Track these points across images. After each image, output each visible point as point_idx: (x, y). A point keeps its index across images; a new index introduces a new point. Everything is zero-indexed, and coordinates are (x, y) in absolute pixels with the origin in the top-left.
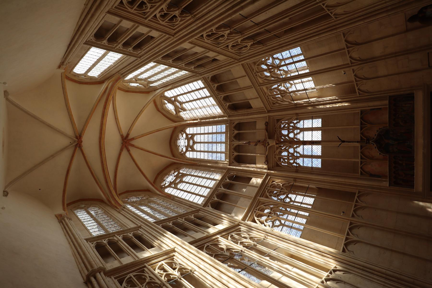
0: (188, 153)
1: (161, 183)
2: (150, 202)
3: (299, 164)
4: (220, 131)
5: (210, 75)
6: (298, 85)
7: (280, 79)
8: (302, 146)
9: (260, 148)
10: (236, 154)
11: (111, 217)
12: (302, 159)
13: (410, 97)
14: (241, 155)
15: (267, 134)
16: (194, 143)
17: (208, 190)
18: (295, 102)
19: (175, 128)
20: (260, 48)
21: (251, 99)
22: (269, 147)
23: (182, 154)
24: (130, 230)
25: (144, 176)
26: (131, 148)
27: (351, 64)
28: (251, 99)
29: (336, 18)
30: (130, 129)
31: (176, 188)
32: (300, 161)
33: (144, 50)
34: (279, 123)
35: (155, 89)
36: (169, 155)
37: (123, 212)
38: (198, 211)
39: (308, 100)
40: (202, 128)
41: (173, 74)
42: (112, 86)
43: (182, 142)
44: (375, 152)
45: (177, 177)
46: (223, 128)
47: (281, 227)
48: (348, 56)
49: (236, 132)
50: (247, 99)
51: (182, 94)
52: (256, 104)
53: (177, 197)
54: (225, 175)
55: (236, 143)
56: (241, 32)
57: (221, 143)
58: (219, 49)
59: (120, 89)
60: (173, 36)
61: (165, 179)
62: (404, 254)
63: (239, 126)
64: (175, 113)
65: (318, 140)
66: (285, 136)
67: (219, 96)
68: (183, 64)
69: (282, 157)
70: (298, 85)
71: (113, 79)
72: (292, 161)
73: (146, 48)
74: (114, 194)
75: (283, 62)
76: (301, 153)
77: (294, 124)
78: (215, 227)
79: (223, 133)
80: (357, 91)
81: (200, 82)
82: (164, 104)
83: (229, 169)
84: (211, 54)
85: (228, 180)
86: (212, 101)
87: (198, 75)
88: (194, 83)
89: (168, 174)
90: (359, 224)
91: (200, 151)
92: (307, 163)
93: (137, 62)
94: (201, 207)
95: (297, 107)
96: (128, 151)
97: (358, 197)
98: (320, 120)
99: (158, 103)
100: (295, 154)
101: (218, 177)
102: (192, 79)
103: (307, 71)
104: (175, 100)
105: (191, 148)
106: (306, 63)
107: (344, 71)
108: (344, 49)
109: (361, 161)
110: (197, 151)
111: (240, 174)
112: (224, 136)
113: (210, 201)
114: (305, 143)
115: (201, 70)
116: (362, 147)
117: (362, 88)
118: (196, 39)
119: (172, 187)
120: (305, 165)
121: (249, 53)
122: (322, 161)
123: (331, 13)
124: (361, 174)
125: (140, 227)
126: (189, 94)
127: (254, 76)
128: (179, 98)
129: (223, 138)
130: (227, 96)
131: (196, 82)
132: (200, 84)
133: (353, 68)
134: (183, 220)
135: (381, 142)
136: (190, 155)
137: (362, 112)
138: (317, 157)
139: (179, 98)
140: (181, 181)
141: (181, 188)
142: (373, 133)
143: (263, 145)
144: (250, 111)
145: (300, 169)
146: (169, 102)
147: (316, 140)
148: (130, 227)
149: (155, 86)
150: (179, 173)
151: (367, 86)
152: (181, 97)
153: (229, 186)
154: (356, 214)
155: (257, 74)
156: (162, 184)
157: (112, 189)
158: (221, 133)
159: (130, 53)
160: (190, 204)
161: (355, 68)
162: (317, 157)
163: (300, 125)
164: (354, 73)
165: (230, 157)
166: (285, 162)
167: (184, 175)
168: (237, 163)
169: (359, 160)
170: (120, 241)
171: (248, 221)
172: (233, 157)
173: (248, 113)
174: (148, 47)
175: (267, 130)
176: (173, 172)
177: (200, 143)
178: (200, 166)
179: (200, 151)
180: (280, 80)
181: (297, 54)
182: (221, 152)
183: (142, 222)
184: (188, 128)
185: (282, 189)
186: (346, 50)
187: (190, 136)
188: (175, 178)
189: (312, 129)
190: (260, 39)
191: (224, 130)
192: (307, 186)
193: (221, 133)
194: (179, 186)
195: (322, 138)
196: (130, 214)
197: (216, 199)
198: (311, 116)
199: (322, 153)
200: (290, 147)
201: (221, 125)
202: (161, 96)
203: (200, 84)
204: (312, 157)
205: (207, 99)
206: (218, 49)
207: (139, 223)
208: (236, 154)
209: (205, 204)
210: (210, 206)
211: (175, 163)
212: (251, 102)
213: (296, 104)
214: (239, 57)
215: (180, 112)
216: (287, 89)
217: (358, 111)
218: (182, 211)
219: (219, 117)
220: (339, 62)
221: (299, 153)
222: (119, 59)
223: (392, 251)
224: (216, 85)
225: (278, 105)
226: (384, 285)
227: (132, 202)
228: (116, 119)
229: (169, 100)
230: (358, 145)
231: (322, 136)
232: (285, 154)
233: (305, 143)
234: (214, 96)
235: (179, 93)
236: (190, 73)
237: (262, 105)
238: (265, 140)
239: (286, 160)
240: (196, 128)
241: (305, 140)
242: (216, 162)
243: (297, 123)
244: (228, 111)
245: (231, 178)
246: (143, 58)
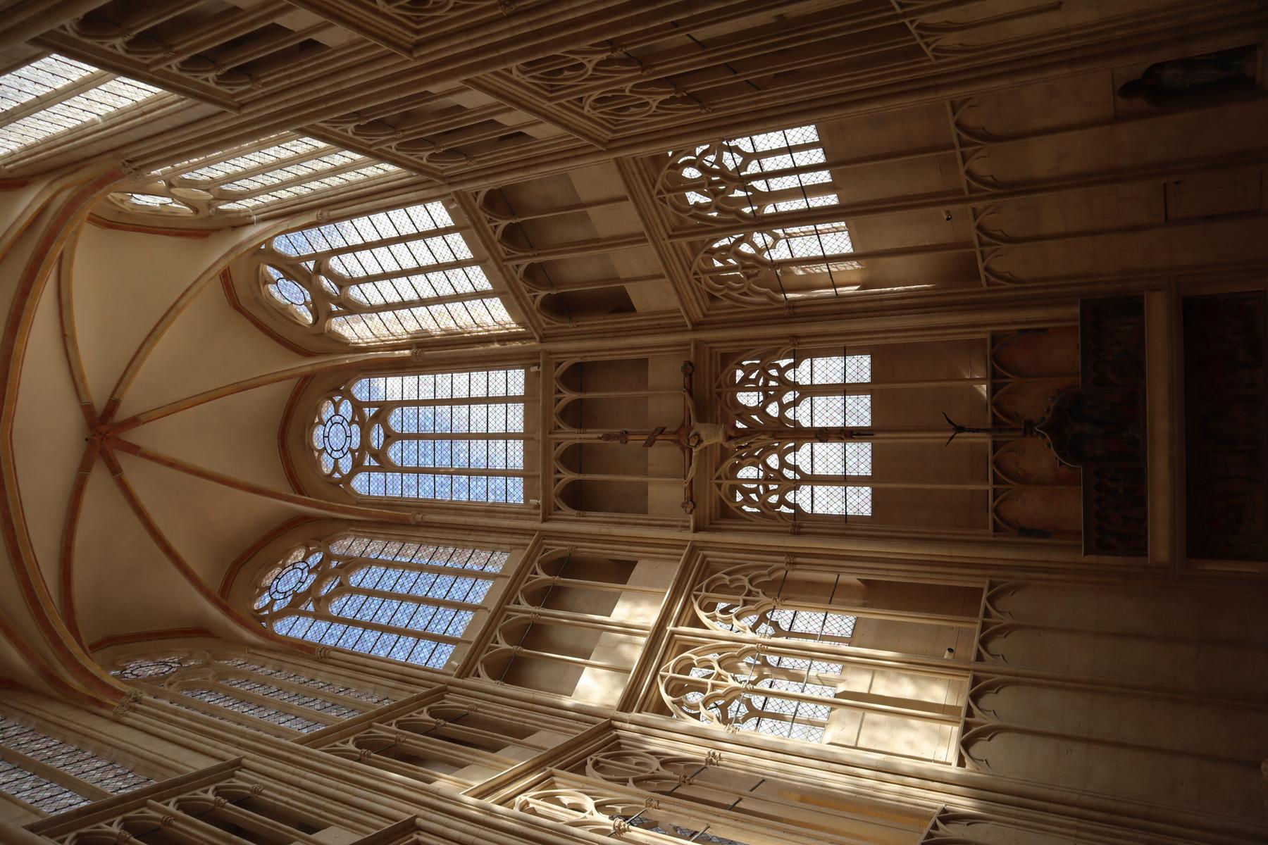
0: (362, 477)
1: (253, 599)
2: (223, 675)
3: (795, 506)
4: (501, 392)
5: (484, 186)
6: (803, 244)
7: (744, 216)
8: (806, 447)
9: (663, 454)
10: (568, 476)
11: (83, 739)
12: (808, 488)
13: (1132, 306)
14: (589, 481)
15: (690, 404)
16: (390, 437)
17: (468, 616)
18: (789, 296)
19: (306, 380)
20: (688, 114)
21: (635, 279)
22: (704, 452)
23: (336, 484)
24: (201, 778)
25: (187, 572)
26: (127, 463)
27: (971, 192)
28: (635, 279)
29: (937, 57)
30: (122, 382)
31: (321, 615)
32: (802, 498)
33: (264, 85)
34: (732, 365)
35: (239, 222)
36: (283, 487)
37: (132, 718)
38: (441, 693)
39: (831, 291)
40: (427, 379)
41: (335, 171)
42: (71, 207)
43: (333, 436)
44: (1039, 456)
45: (322, 572)
46: (516, 381)
47: (754, 720)
48: (962, 170)
49: (569, 396)
50: (618, 280)
51: (352, 249)
52: (650, 297)
53: (335, 649)
54: (528, 556)
55: (570, 436)
56: (641, 61)
57: (506, 436)
58: (552, 104)
59: (95, 220)
60: (410, 52)
61: (267, 582)
62: (1119, 745)
63: (578, 375)
64: (310, 319)
65: (862, 424)
66: (744, 412)
67: (511, 264)
68: (394, 144)
69: (737, 486)
70: (803, 244)
71: (84, 175)
72: (774, 499)
73: (275, 79)
74: (75, 649)
75: (755, 162)
76: (806, 469)
77: (782, 371)
78: (527, 740)
79: (515, 400)
80: (982, 273)
81: (437, 208)
82: (266, 283)
83: (544, 535)
84: (512, 119)
85: (543, 576)
87: (439, 182)
88: (410, 210)
89: (277, 560)
90: (998, 678)
91: (419, 470)
92: (827, 502)
93: (219, 124)
94: (453, 679)
95: (795, 315)
96: (115, 471)
97: (990, 599)
98: (866, 360)
99: (239, 280)
100: (789, 474)
101: (498, 562)
102: (411, 196)
103: (831, 200)
104: (318, 271)
105: (376, 455)
106: (831, 173)
107: (948, 212)
108: (952, 147)
109: (995, 490)
110: (403, 470)
111: (586, 550)
112: (517, 411)
113: (483, 656)
114: (824, 435)
115: (454, 166)
116: (996, 446)
117: (998, 266)
118: (496, 73)
119: (306, 614)
120: (818, 510)
121: (647, 125)
122: (873, 494)
123: (928, 45)
124: (996, 528)
125: (238, 764)
126: (384, 250)
127: (653, 202)
128: (334, 263)
129: (516, 418)
130: (541, 264)
131: (420, 208)
132: (439, 214)
133: (973, 204)
134: (394, 728)
135: (1062, 428)
136: (368, 485)
137: (995, 338)
138: (858, 481)
139: (334, 263)
140: (343, 589)
141: (349, 613)
142: (1034, 401)
143: (676, 442)
144: (625, 320)
145: (802, 523)
146: (288, 277)
147: (854, 424)
148: (193, 771)
149: (239, 211)
150: (328, 557)
151: (1010, 261)
152: (348, 258)
153: (550, 597)
154: (986, 650)
155: (667, 195)
156: (258, 605)
157: (61, 628)
158: (506, 400)
159: (205, 88)
160: (405, 675)
161: (979, 205)
162: (858, 481)
163: (802, 374)
164: (976, 218)
165: (545, 489)
166: (751, 503)
167: (351, 564)
168: (575, 512)
169: (989, 487)
170: (177, 818)
171: (639, 711)
172: (554, 490)
173: (619, 330)
174: (289, 76)
175: (690, 393)
176: (300, 554)
177: (418, 437)
178: (419, 525)
179: (419, 470)
180: (744, 222)
181: (801, 142)
182: (507, 473)
183: (239, 745)
184: (365, 381)
185: (749, 593)
186: (958, 151)
187: (374, 410)
188: (313, 577)
189: (844, 389)
190: (695, 87)
191: (517, 388)
192: (831, 577)
193: (506, 400)
194: (334, 609)
195: (873, 420)
196: (171, 722)
197: (503, 645)
198: (842, 344)
199: (873, 469)
200: (769, 450)
201: (506, 368)
202: (257, 251)
203: (439, 214)
204: (844, 480)
205: (459, 271)
206: (547, 105)
207: (231, 754)
208: (568, 476)
209: (465, 671)
210: (482, 672)
211: (304, 520)
212: (632, 290)
213: (793, 304)
214: (611, 136)
215: (332, 314)
216: (760, 251)
217: (984, 334)
218: (373, 699)
219: (502, 339)
220: (927, 179)
221: (795, 468)
222: (138, 105)
223: (1089, 741)
224: (503, 223)
225: (728, 302)
226: (1076, 836)
227: (144, 680)
228: (66, 336)
229: (292, 269)
230: (984, 439)
231: (873, 414)
232: (748, 472)
233: (824, 435)
234: (491, 263)
235: (339, 243)
236: (404, 173)
237: (674, 303)
238: (683, 425)
239: (754, 496)
240: (398, 379)
241: (816, 425)
242: (491, 510)
243: (788, 367)
244: (540, 317)
246: (250, 114)
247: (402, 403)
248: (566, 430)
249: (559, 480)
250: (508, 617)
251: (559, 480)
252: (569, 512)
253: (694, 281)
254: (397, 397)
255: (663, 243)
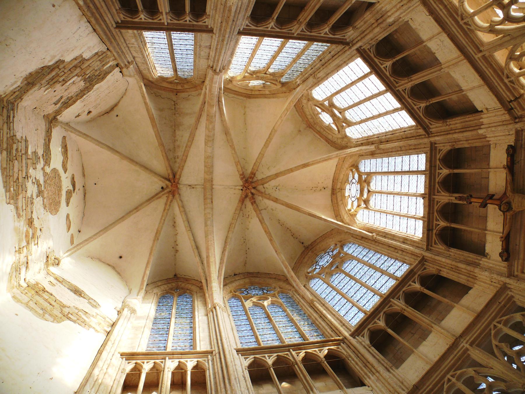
46: (419, 161)
83: (423, 260)
86: (390, 101)
129: (419, 184)
146: (323, 111)
153: (417, 300)
177: (381, 193)
193: (417, 172)
208: (443, 224)
209: (358, 331)
245: (425, 281)
247: (376, 173)
248: (443, 194)
249: (439, 225)
250: (391, 306)
251: (439, 225)
252: (441, 247)
253: (508, 84)
254: (373, 170)
255: (476, 57)
